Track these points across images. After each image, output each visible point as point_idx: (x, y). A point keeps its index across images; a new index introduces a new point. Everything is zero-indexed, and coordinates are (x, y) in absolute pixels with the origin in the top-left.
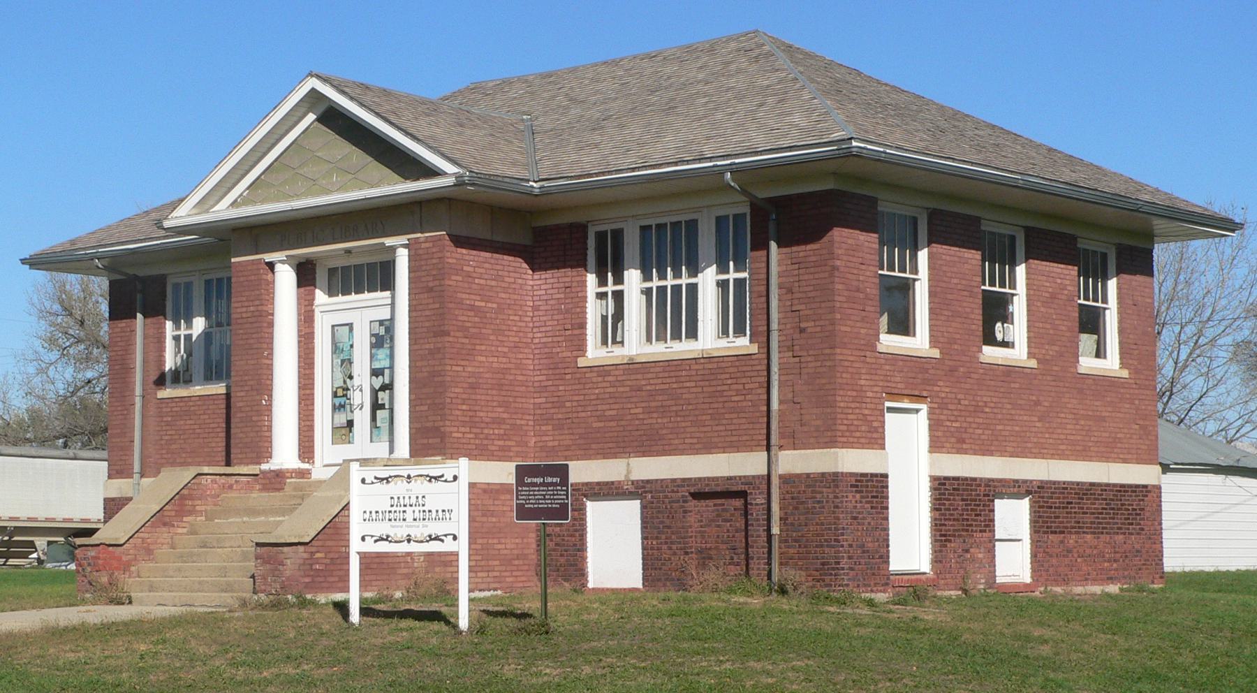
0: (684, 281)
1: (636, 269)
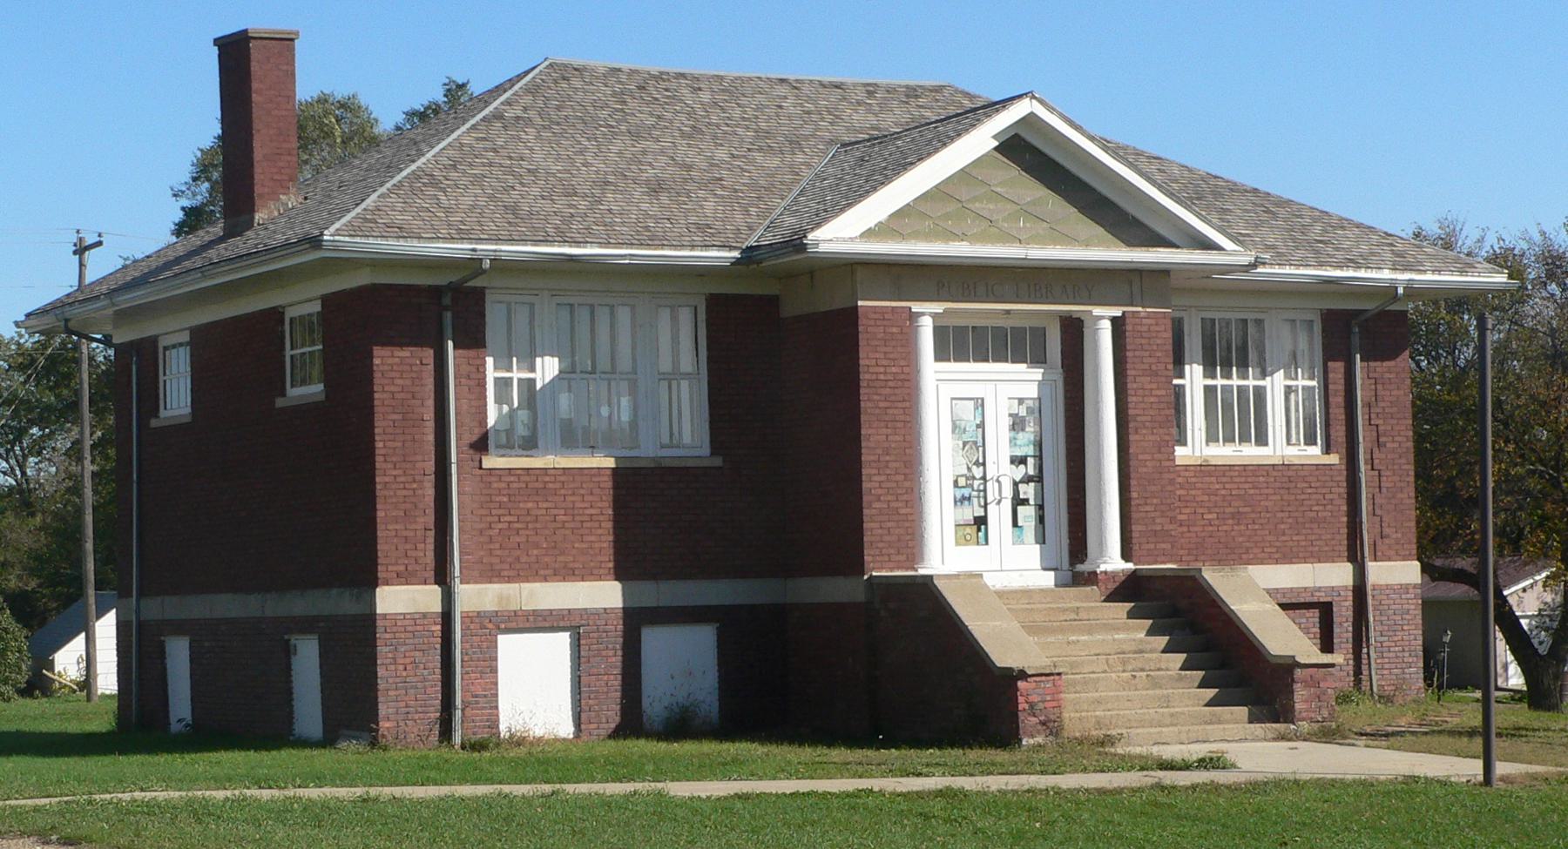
0: (1251, 383)
1: (1199, 364)
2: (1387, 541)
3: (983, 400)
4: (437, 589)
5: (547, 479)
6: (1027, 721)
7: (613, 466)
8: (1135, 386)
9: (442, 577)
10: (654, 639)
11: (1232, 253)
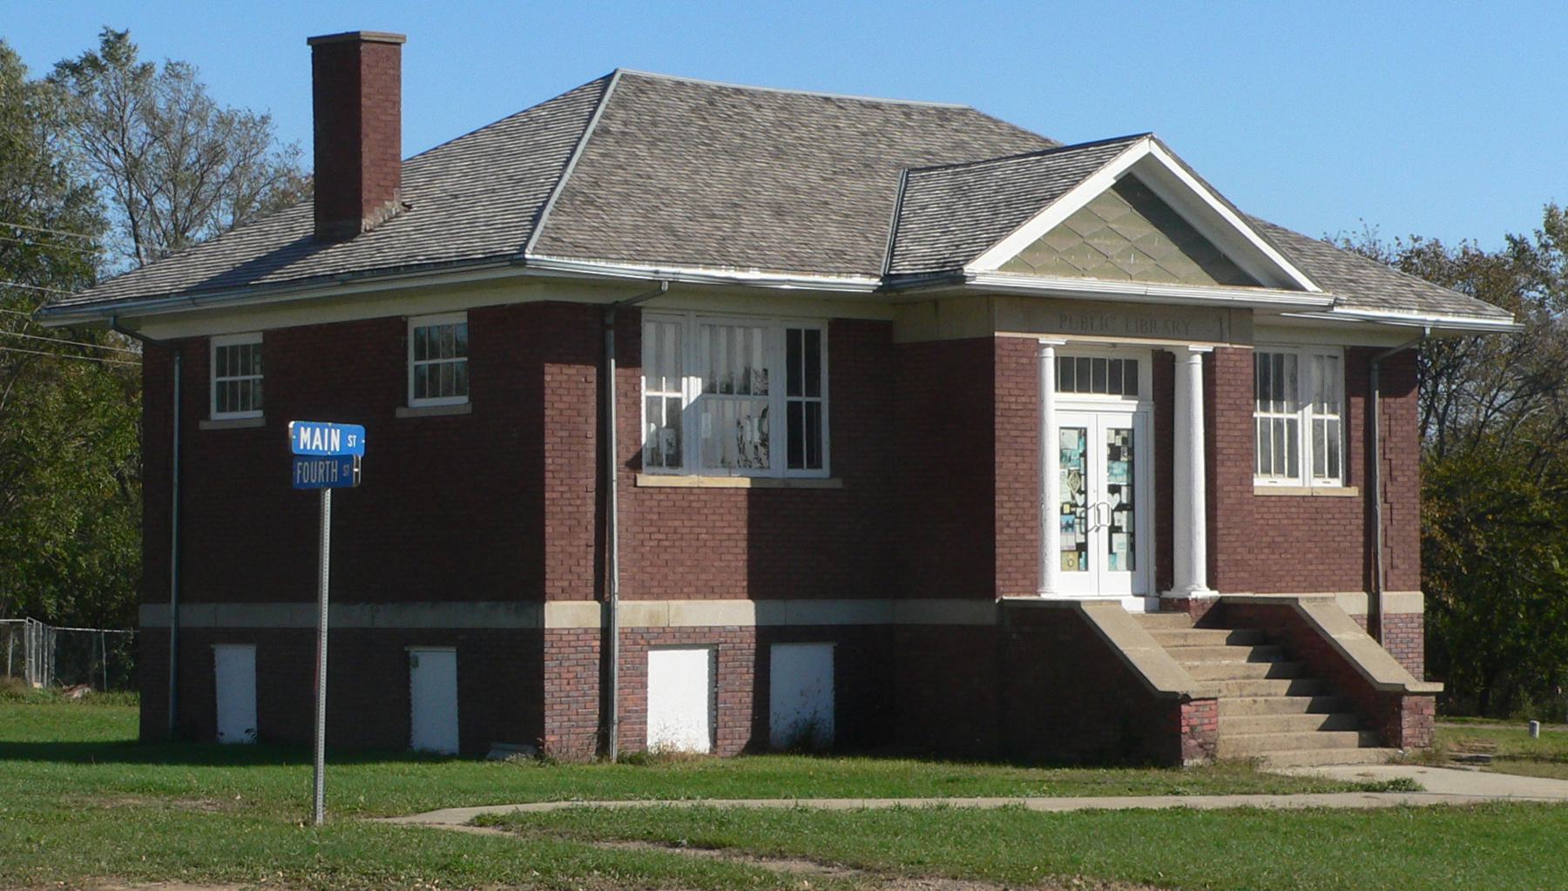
2: (1396, 571)
3: (1085, 429)
4: (596, 605)
5: (692, 498)
6: (1189, 743)
7: (748, 486)
8: (1222, 419)
9: (601, 592)
10: (782, 656)
11: (1312, 293)
